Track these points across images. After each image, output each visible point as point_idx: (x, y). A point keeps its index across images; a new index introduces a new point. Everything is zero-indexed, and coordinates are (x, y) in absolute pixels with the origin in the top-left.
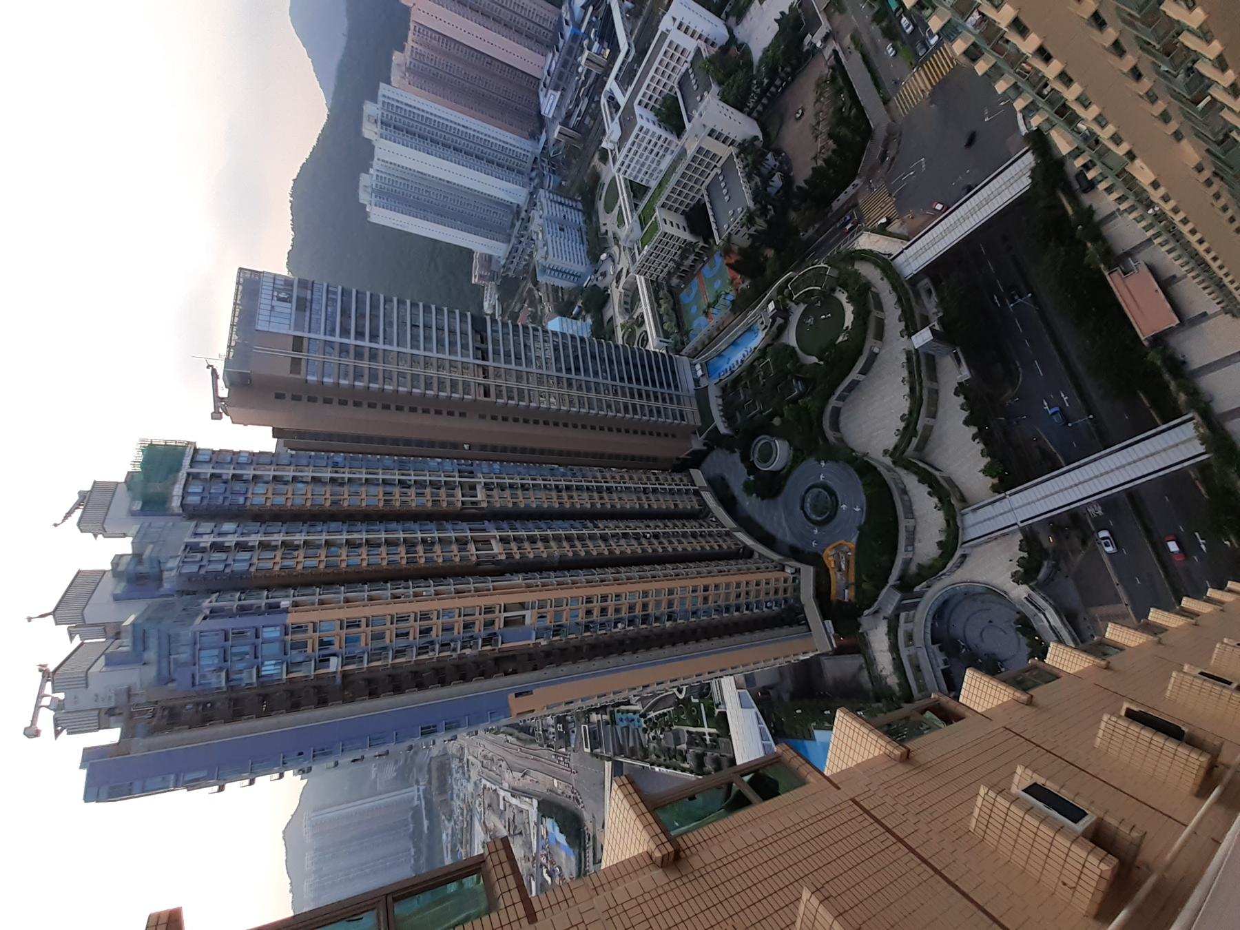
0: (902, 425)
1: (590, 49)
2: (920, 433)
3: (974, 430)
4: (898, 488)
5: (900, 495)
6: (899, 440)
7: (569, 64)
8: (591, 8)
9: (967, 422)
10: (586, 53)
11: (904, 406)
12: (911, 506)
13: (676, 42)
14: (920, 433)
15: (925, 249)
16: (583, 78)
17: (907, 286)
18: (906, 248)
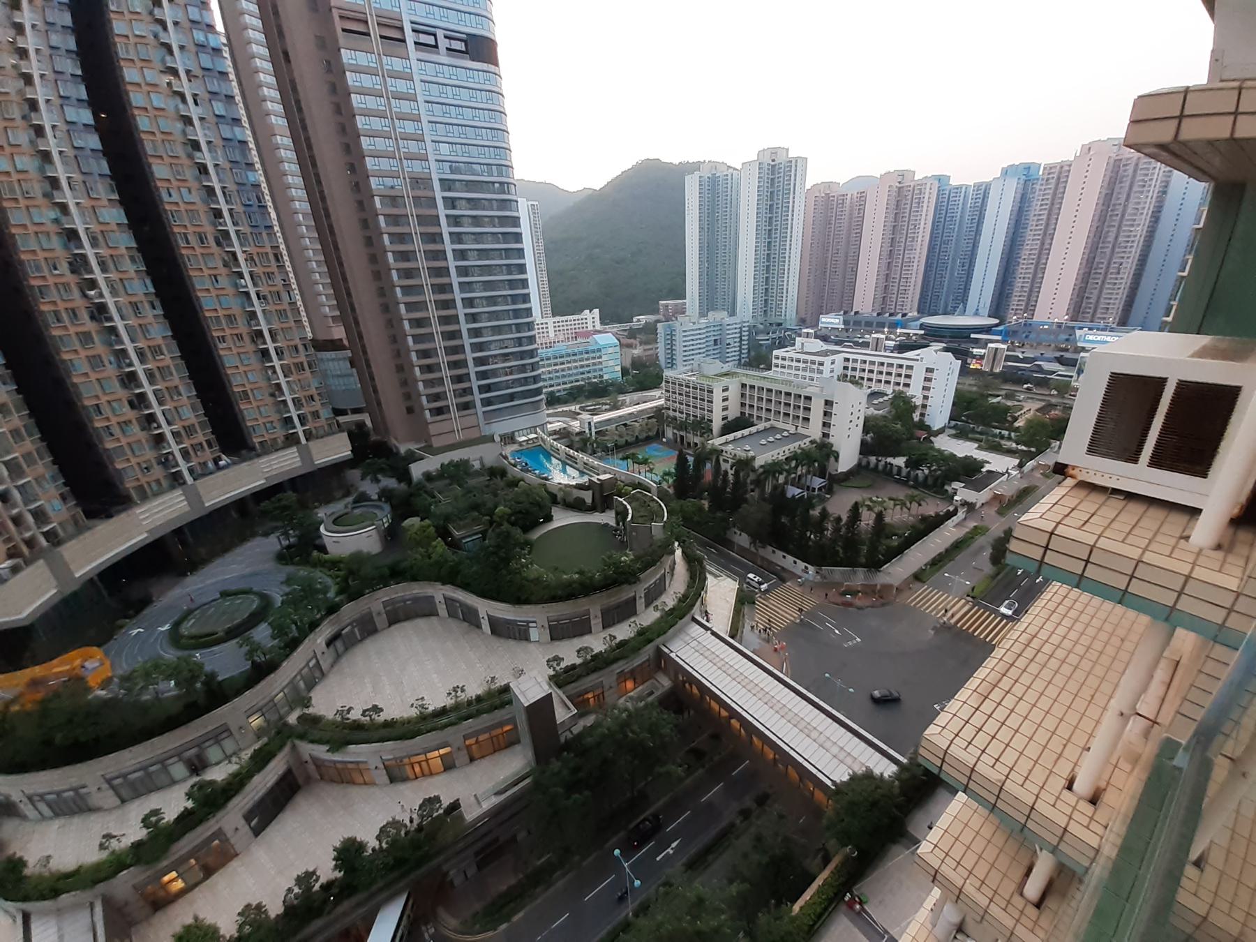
0: (355, 715)
1: (887, 339)
2: (337, 757)
3: (327, 871)
4: (200, 744)
5: (178, 753)
6: (334, 723)
7: (870, 325)
8: (922, 332)
9: (349, 853)
10: (883, 336)
11: (397, 708)
12: (158, 789)
13: (914, 373)
14: (337, 757)
15: (724, 668)
16: (861, 341)
17: (648, 652)
18: (714, 634)
